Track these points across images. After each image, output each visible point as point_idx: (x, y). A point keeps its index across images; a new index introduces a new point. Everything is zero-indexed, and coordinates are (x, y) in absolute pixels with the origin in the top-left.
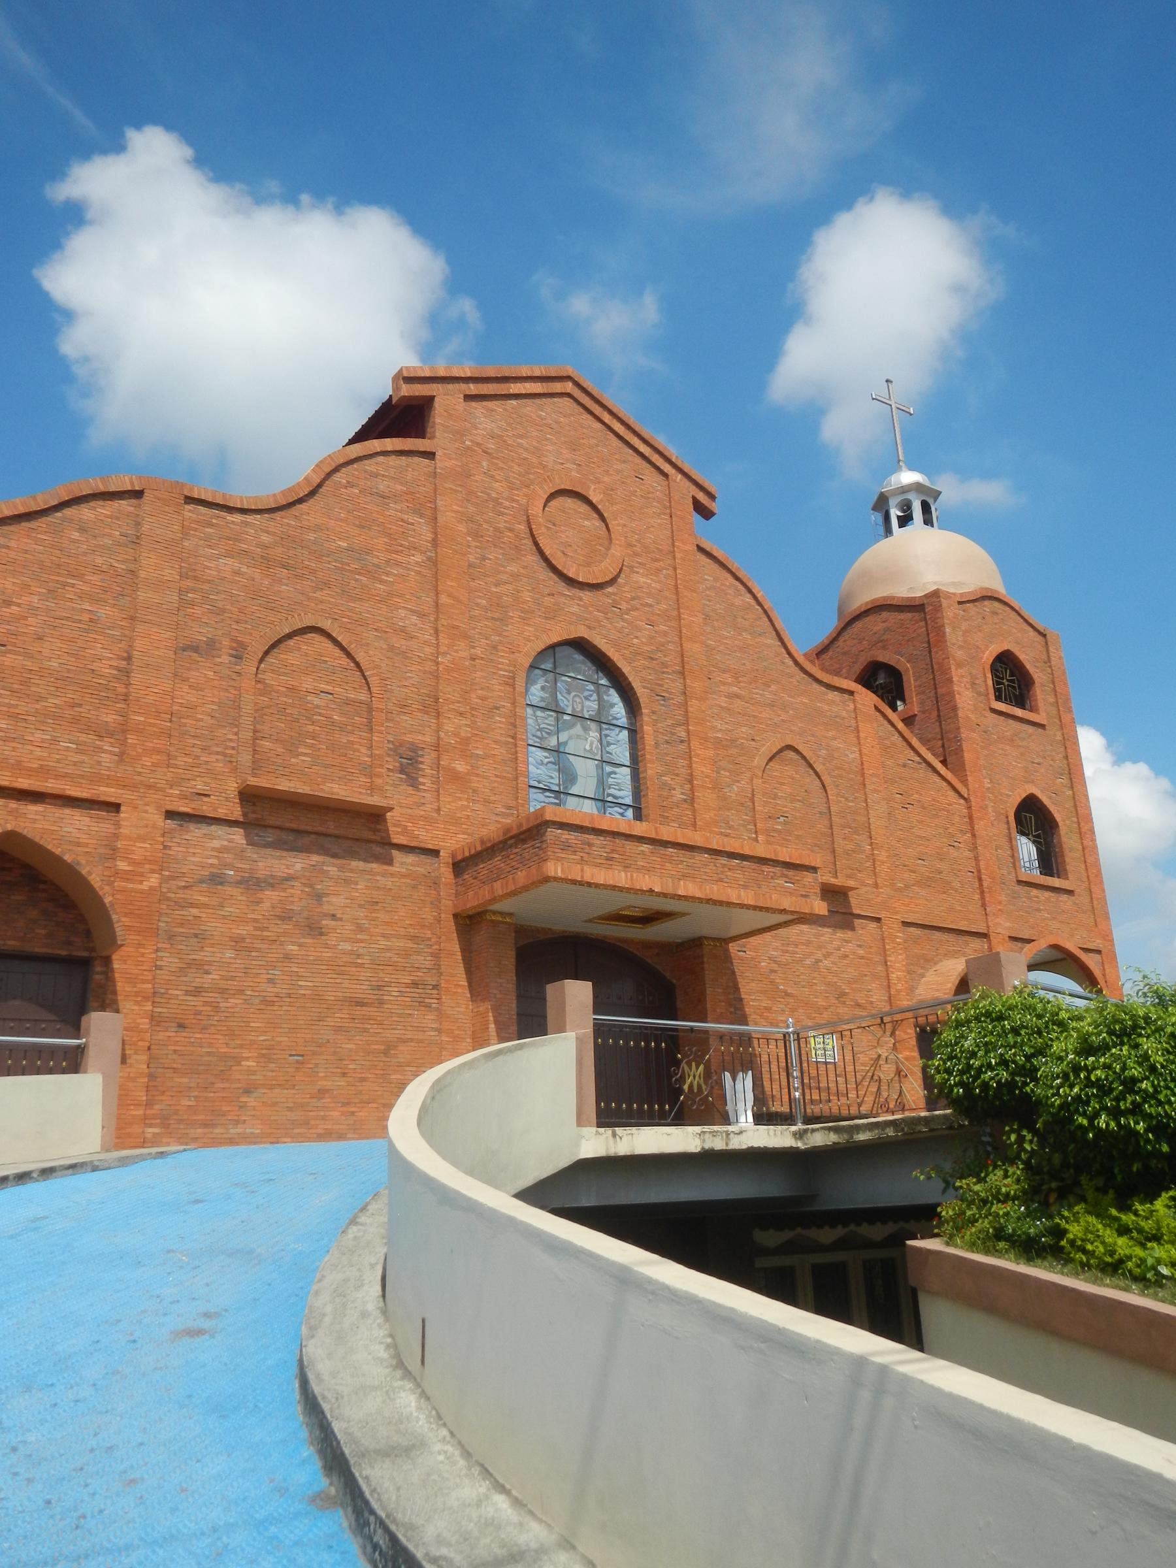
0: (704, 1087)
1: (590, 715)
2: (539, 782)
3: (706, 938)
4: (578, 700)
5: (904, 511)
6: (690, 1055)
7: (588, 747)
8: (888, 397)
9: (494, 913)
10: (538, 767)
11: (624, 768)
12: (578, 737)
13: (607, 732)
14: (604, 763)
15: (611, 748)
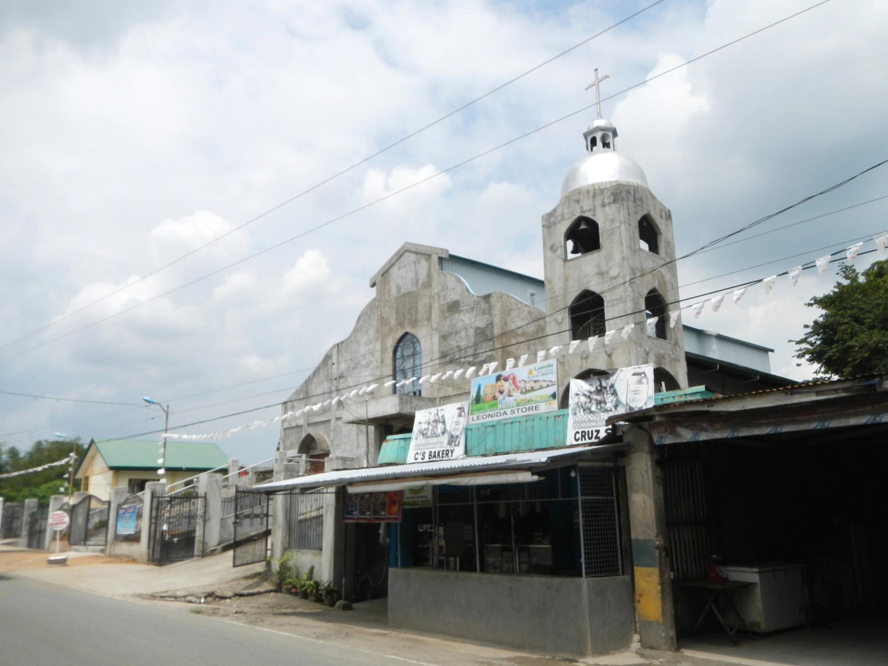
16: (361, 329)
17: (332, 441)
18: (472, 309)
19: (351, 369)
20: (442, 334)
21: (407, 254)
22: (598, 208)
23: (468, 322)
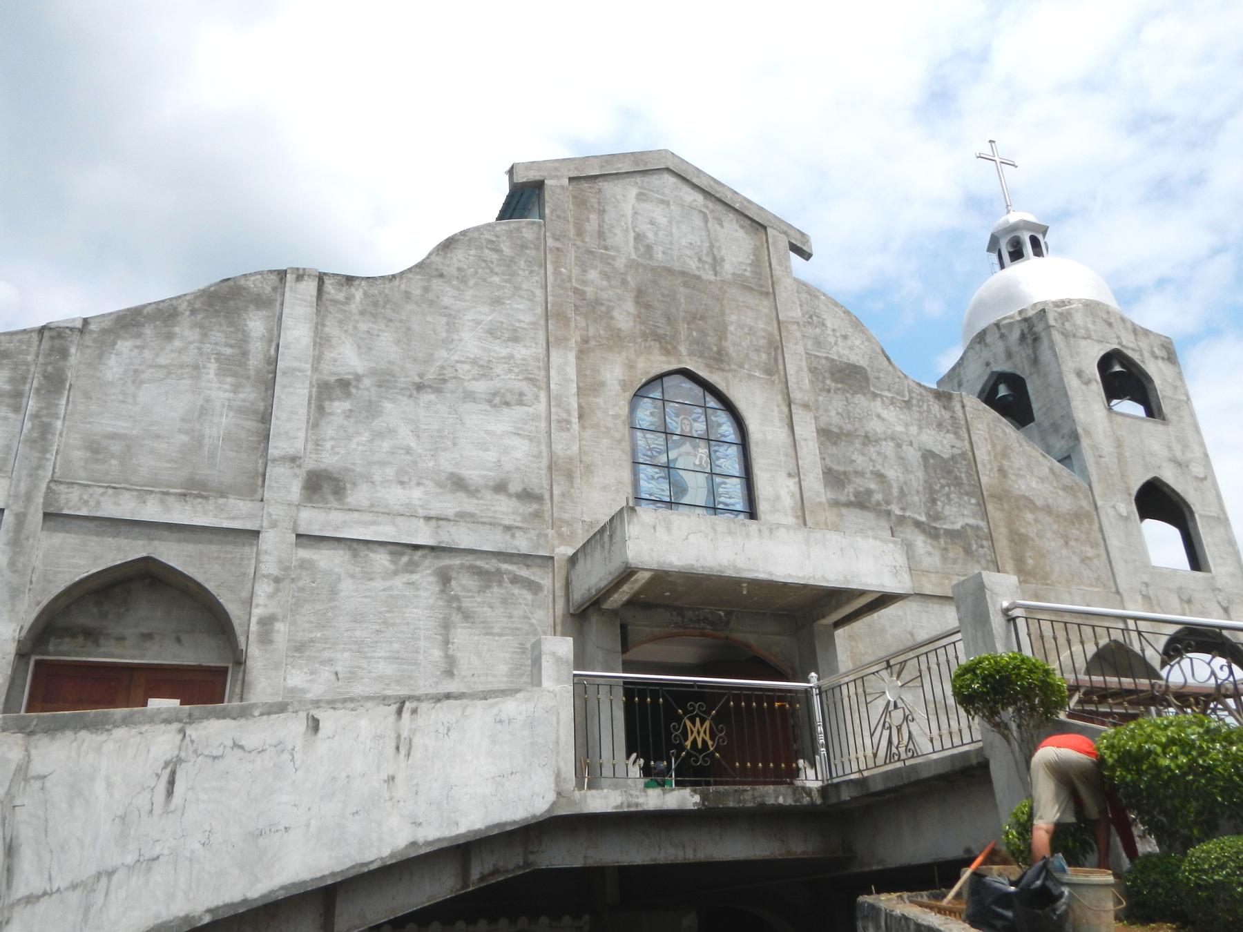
0: (710, 743)
2: (651, 495)
4: (686, 422)
5: (1014, 246)
6: (694, 710)
7: (697, 462)
8: (992, 154)
12: (688, 454)
13: (716, 448)
14: (714, 476)
16: (464, 280)
17: (267, 623)
18: (908, 404)
19: (402, 381)
20: (822, 425)
21: (670, 180)
22: (1146, 354)
23: (900, 428)
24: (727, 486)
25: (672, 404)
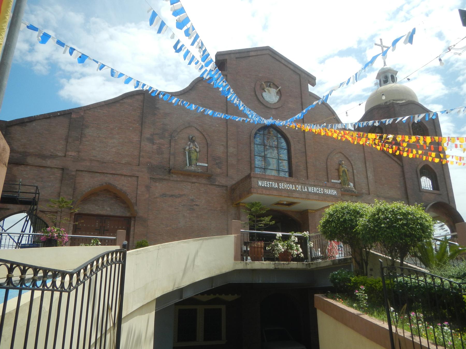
1: (275, 146)
2: (259, 166)
3: (309, 210)
9: (242, 203)
10: (258, 162)
11: (285, 161)
13: (280, 151)
14: (279, 160)
15: (281, 155)
24: (283, 163)
25: (266, 136)
